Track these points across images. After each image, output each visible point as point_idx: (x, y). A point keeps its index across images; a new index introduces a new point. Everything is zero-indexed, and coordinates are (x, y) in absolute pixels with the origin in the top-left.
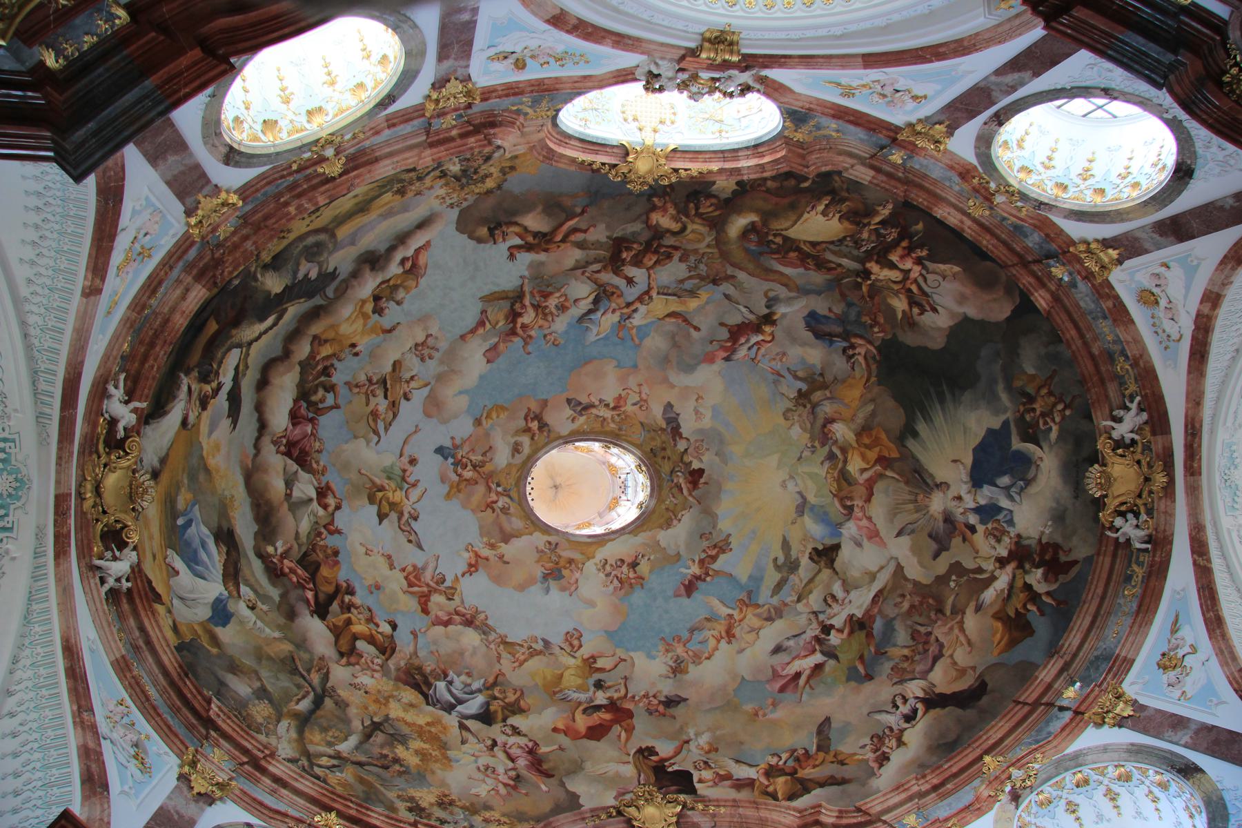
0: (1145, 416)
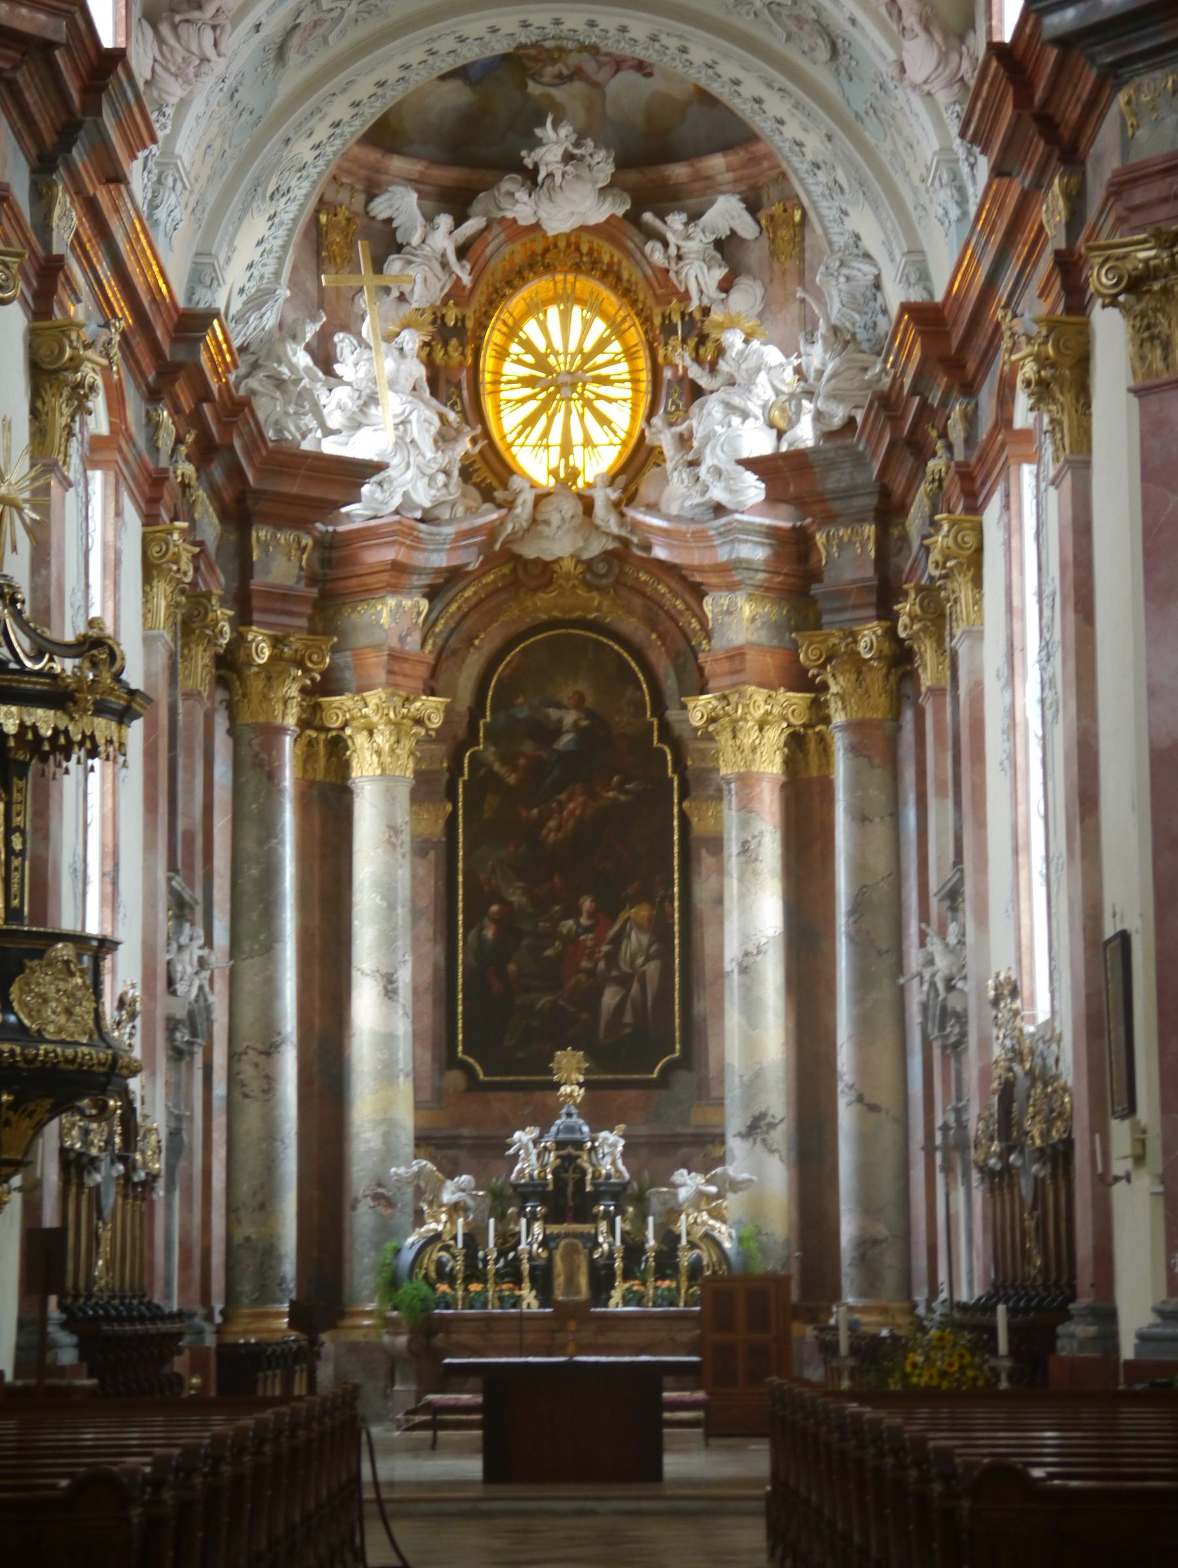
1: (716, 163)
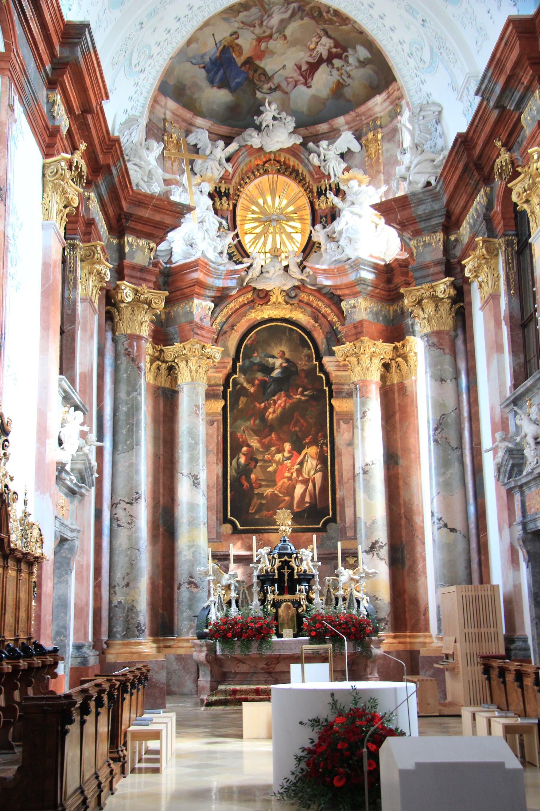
1: (341, 120)
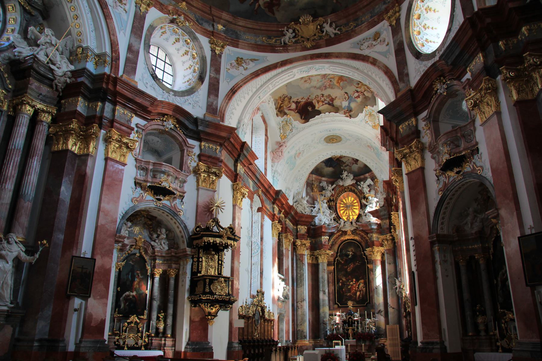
0: (333, 36)
1: (367, 175)
